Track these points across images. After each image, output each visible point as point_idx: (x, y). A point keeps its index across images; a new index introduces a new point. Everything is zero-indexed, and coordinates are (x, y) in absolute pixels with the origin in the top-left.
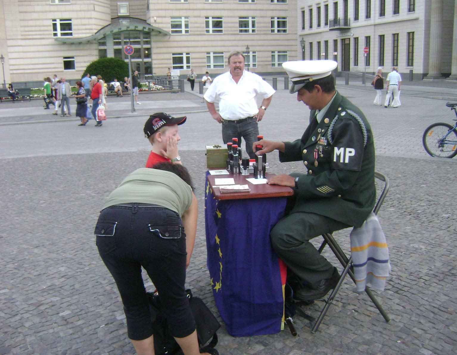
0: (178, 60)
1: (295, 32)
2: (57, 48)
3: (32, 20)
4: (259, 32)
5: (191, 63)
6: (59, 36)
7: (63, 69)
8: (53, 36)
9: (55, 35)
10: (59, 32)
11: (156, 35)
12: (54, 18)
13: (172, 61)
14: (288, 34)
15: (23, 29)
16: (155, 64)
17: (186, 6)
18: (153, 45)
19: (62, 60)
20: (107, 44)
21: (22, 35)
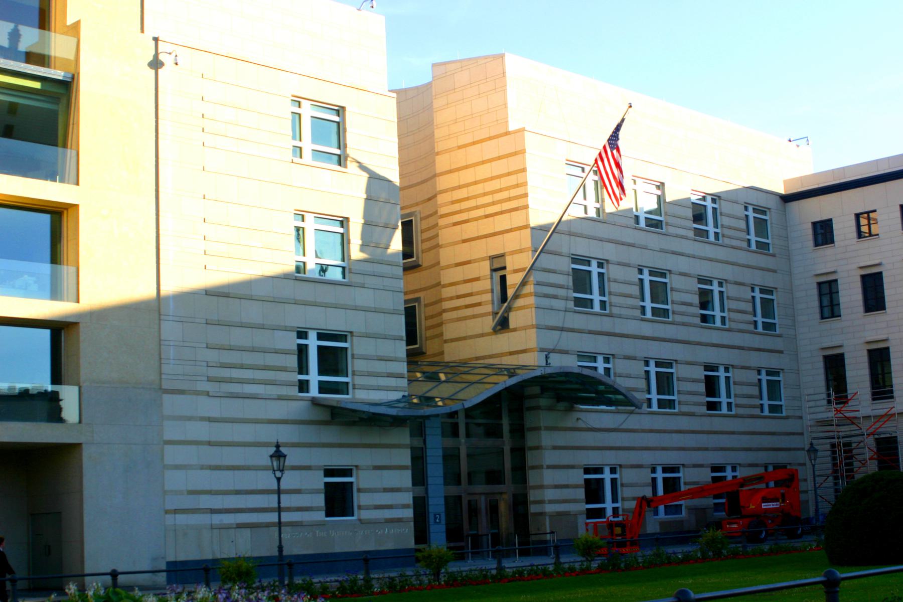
0: (593, 491)
1: (798, 414)
2: (311, 434)
3: (242, 325)
4: (741, 411)
5: (623, 499)
6: (314, 391)
7: (320, 516)
8: (294, 391)
9: (303, 386)
10: (314, 377)
11: (550, 409)
12: (301, 324)
13: (581, 494)
14: (787, 418)
15: (213, 356)
16: (551, 502)
17: (606, 324)
18: (547, 439)
19: (319, 480)
20: (428, 431)
21: (209, 380)
